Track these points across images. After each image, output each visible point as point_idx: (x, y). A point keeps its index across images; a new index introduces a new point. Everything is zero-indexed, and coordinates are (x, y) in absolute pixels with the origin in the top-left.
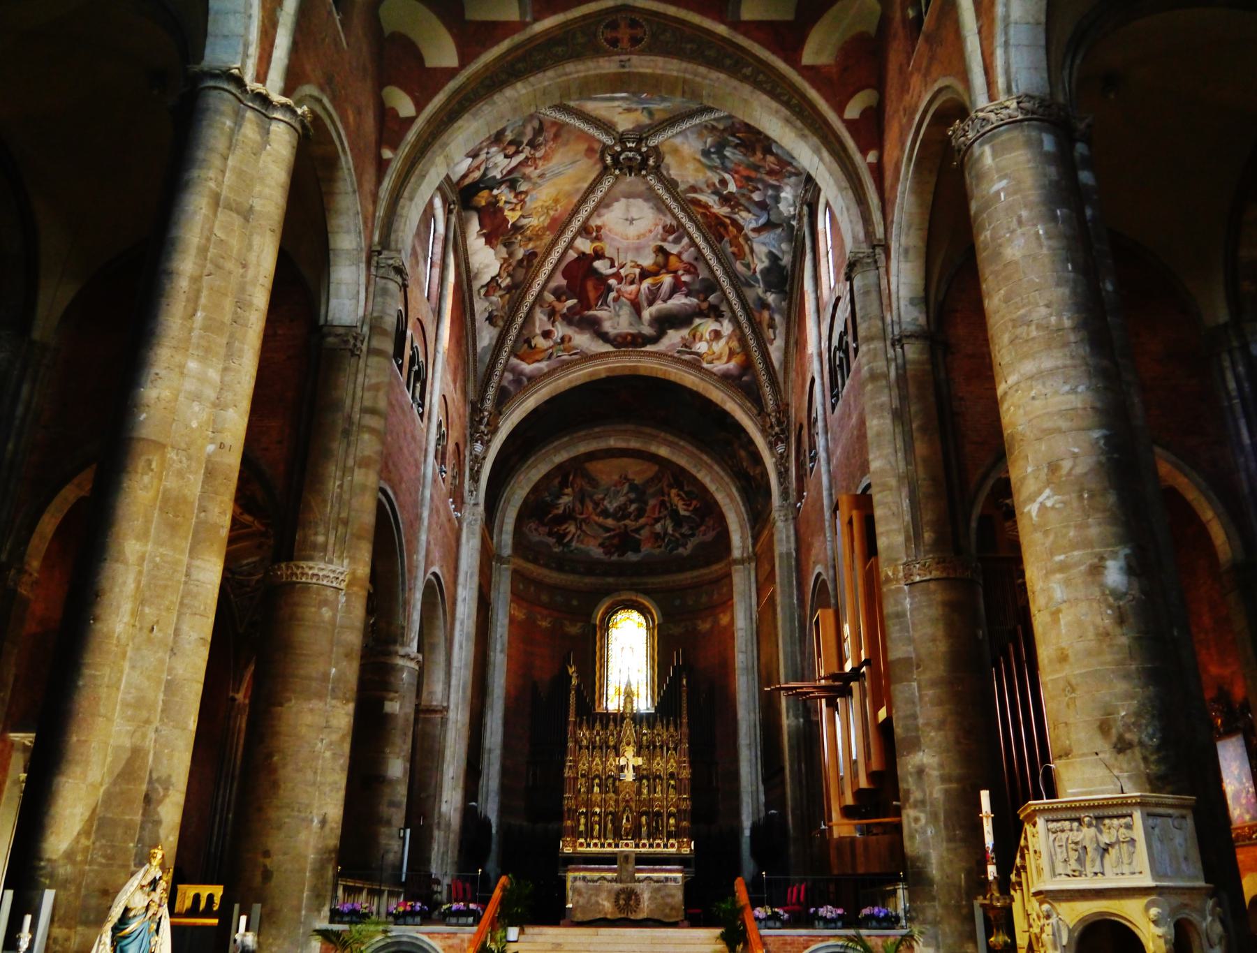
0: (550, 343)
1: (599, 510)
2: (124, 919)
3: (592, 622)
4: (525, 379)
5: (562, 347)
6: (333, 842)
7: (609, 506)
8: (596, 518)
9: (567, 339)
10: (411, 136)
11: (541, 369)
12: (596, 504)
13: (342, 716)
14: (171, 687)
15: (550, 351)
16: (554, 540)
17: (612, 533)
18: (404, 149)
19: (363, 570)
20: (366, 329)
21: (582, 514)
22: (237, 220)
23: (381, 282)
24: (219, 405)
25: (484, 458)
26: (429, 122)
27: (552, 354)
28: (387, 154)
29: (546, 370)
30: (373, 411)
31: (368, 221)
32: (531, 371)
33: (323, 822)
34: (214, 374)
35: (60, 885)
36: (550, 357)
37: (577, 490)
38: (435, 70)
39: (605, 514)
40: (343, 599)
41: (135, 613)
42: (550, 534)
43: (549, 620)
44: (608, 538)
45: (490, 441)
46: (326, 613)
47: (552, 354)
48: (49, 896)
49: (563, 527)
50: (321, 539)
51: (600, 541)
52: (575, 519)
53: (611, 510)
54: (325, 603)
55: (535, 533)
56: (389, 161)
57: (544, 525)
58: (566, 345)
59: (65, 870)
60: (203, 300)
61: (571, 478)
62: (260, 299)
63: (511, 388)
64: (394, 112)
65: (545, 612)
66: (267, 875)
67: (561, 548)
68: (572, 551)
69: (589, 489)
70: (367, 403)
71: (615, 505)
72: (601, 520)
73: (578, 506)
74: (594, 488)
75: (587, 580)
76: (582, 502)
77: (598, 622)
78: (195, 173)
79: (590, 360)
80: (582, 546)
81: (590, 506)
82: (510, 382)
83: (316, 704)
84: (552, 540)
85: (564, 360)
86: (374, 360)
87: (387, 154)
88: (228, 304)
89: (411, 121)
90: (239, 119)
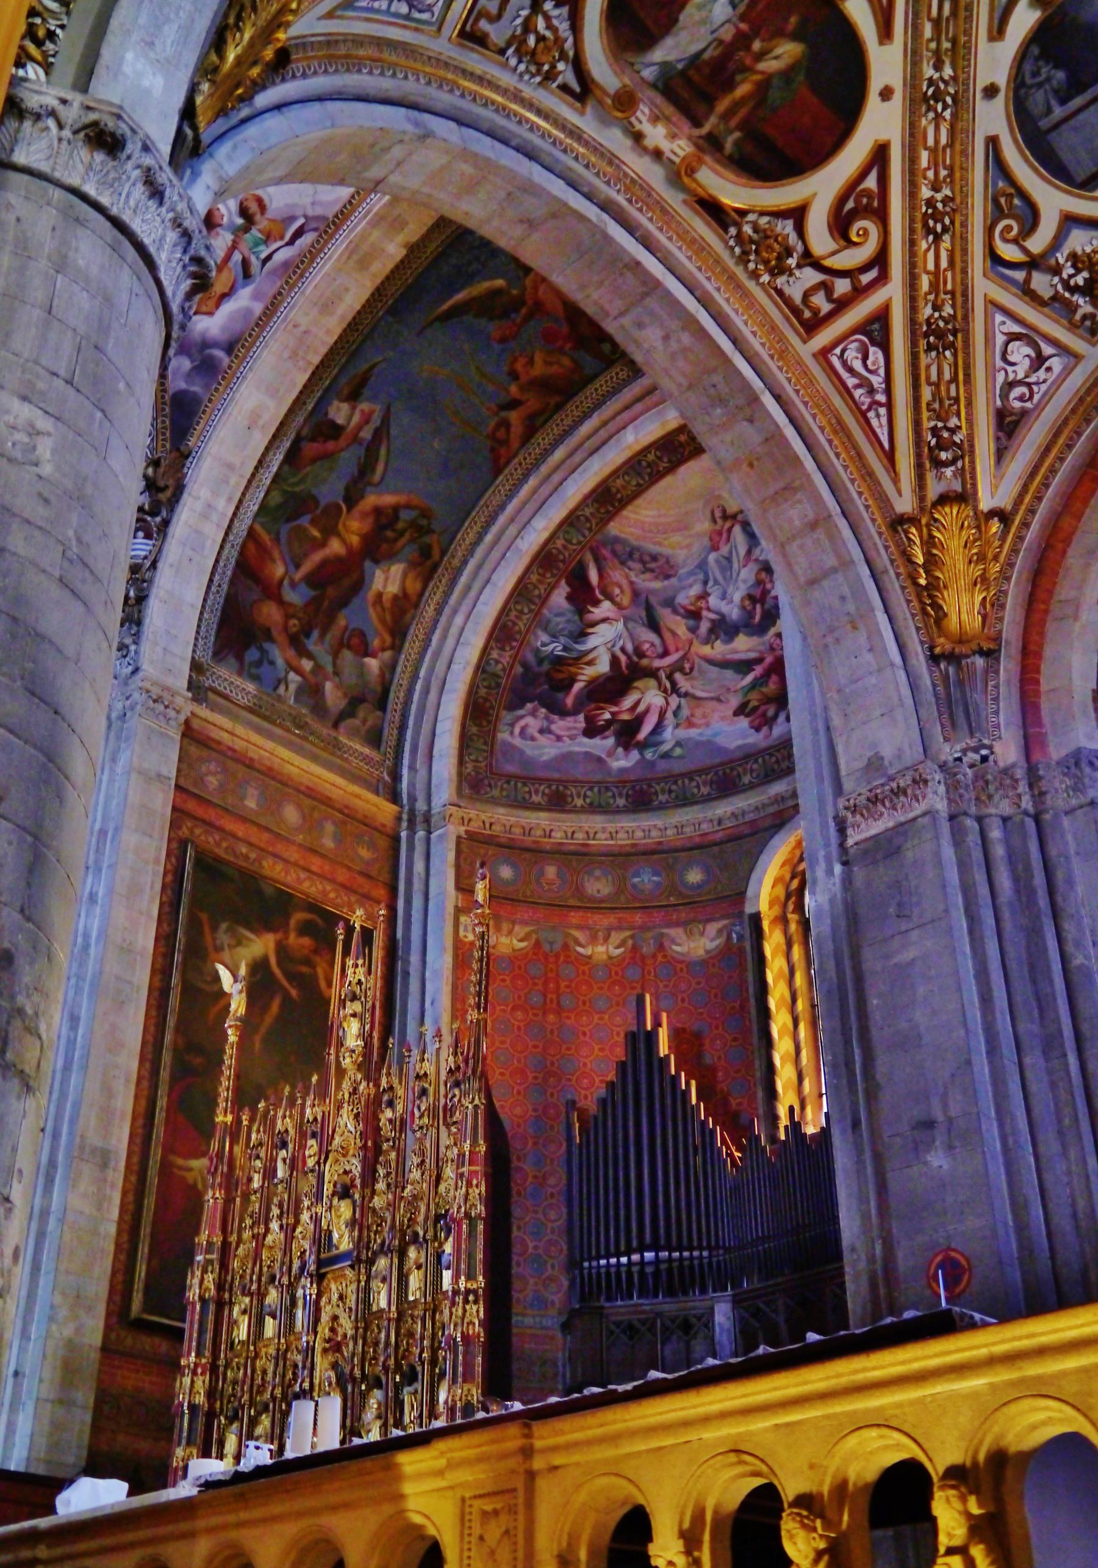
0: (229, 237)
1: (704, 626)
3: (749, 909)
4: (219, 353)
5: (254, 231)
7: (724, 608)
8: (706, 650)
9: (254, 207)
11: (248, 312)
12: (695, 615)
15: (237, 257)
16: (611, 741)
17: (758, 670)
21: (666, 653)
25: (154, 565)
27: (245, 264)
29: (258, 308)
32: (224, 329)
36: (247, 275)
37: (626, 600)
39: (724, 629)
42: (592, 730)
43: (616, 937)
44: (753, 686)
45: (166, 523)
47: (245, 264)
49: (628, 702)
51: (735, 701)
52: (653, 673)
53: (734, 613)
55: (542, 740)
57: (563, 713)
58: (262, 223)
61: (593, 576)
63: (196, 389)
65: (606, 920)
67: (635, 755)
68: (666, 756)
69: (657, 585)
71: (737, 597)
72: (719, 649)
73: (648, 636)
74: (667, 577)
75: (723, 809)
76: (653, 625)
77: (764, 906)
79: (338, 227)
80: (693, 733)
81: (680, 626)
82: (188, 376)
84: (602, 745)
85: (286, 264)
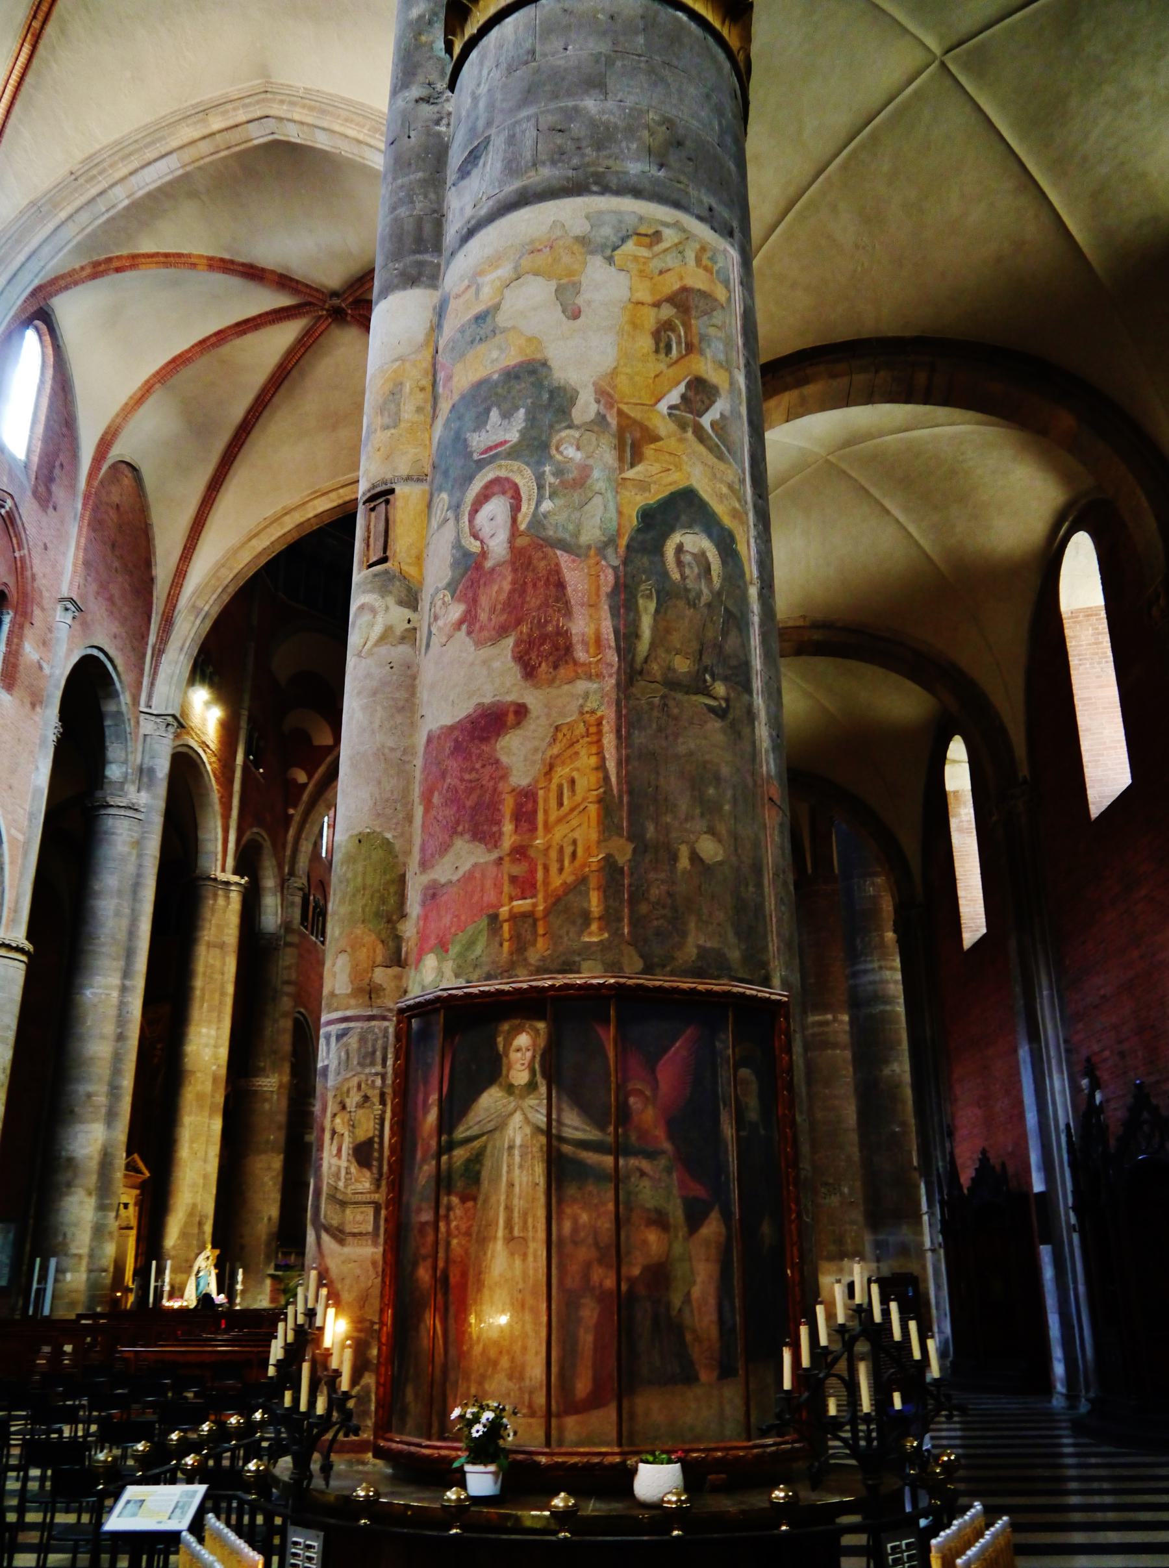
2: (198, 1272)
6: (275, 1229)
10: (305, 797)
13: (276, 1162)
14: (205, 1177)
18: (301, 808)
19: (286, 1079)
20: (282, 931)
22: (218, 951)
23: (290, 898)
24: (216, 1046)
26: (316, 785)
28: (291, 811)
30: (288, 983)
31: (280, 867)
33: (270, 1219)
34: (213, 1032)
35: (172, 1258)
38: (320, 747)
40: (275, 1097)
41: (191, 1148)
46: (267, 1106)
48: (169, 1263)
50: (262, 1064)
54: (266, 1100)
56: (292, 815)
59: (172, 1253)
60: (207, 997)
62: (230, 989)
64: (295, 780)
66: (242, 1247)
70: (286, 978)
78: (200, 934)
83: (263, 1157)
86: (289, 950)
87: (291, 811)
88: (217, 996)
89: (305, 785)
90: (215, 896)
